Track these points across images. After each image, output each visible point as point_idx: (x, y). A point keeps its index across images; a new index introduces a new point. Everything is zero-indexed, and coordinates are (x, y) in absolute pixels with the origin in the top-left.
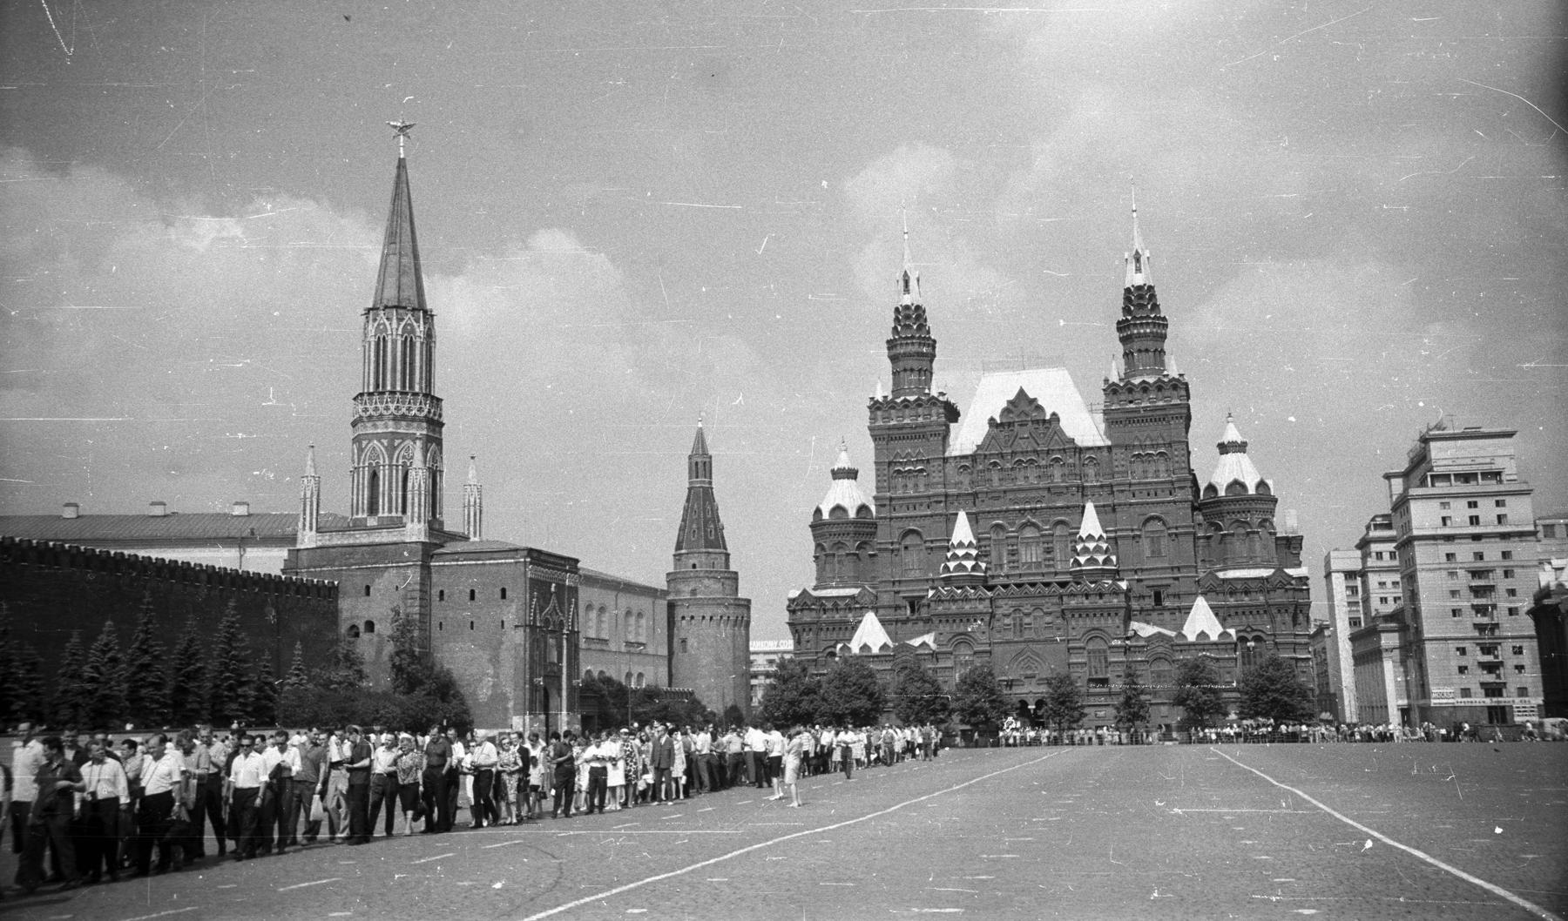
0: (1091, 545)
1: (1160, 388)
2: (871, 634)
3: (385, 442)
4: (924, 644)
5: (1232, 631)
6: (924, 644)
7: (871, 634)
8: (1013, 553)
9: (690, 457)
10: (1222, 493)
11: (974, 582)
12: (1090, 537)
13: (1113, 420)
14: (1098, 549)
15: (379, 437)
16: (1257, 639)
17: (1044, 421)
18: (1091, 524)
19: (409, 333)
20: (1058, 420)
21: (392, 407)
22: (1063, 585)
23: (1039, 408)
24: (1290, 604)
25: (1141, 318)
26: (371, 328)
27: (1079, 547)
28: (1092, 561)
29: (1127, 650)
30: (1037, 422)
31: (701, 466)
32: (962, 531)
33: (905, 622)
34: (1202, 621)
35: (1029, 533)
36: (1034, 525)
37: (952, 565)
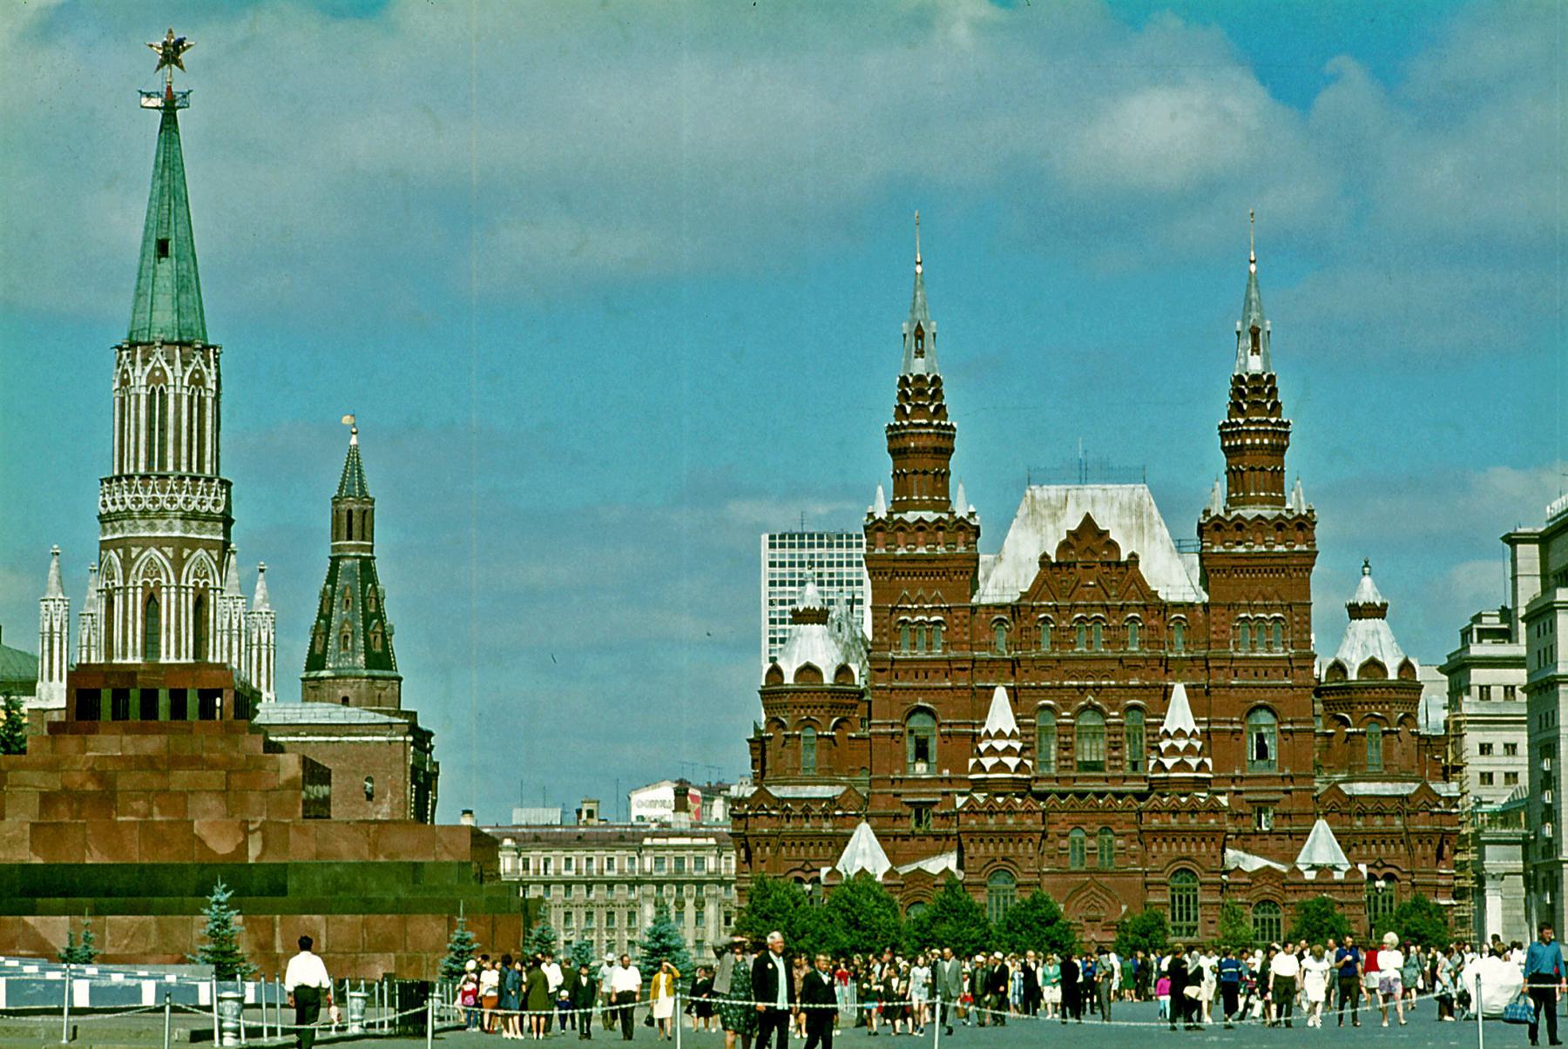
0: (1181, 744)
1: (1280, 527)
3: (169, 551)
5: (1363, 868)
7: (864, 854)
8: (1066, 747)
9: (336, 501)
10: (1353, 676)
11: (1023, 788)
14: (1190, 750)
15: (159, 543)
16: (1389, 878)
17: (1118, 564)
18: (1180, 715)
20: (1137, 562)
21: (180, 498)
22: (1141, 796)
23: (1113, 546)
24: (1436, 832)
26: (139, 376)
27: (1165, 745)
28: (1182, 766)
29: (1223, 888)
30: (1109, 564)
31: (353, 521)
32: (1001, 716)
33: (905, 838)
34: (1321, 847)
35: (1089, 721)
36: (1096, 709)
37: (988, 762)
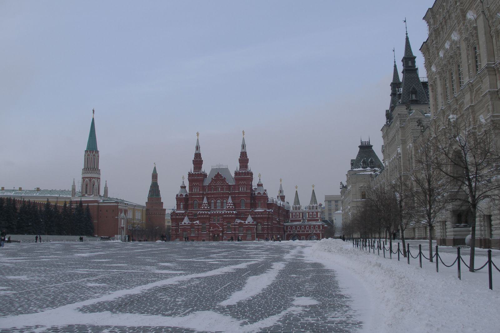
2: (186, 221)
4: (196, 223)
6: (196, 223)
12: (229, 203)
13: (236, 179)
14: (231, 205)
15: (88, 178)
19: (94, 155)
23: (222, 177)
25: (244, 159)
31: (155, 176)
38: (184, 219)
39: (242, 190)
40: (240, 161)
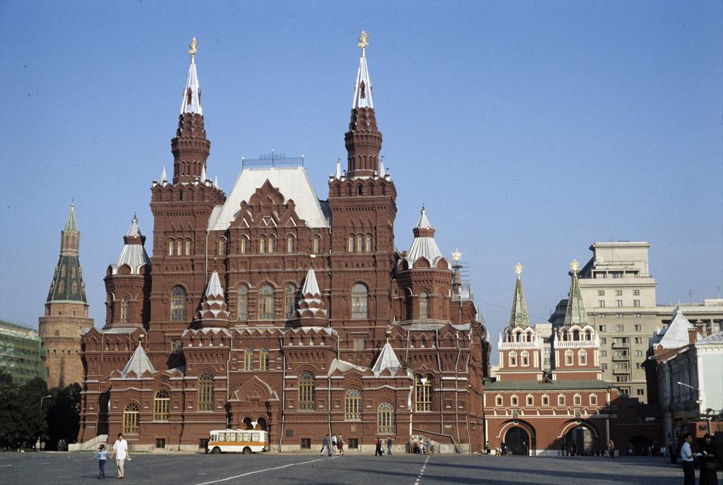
23: (281, 197)
38: (128, 357)
39: (355, 248)
40: (350, 142)
